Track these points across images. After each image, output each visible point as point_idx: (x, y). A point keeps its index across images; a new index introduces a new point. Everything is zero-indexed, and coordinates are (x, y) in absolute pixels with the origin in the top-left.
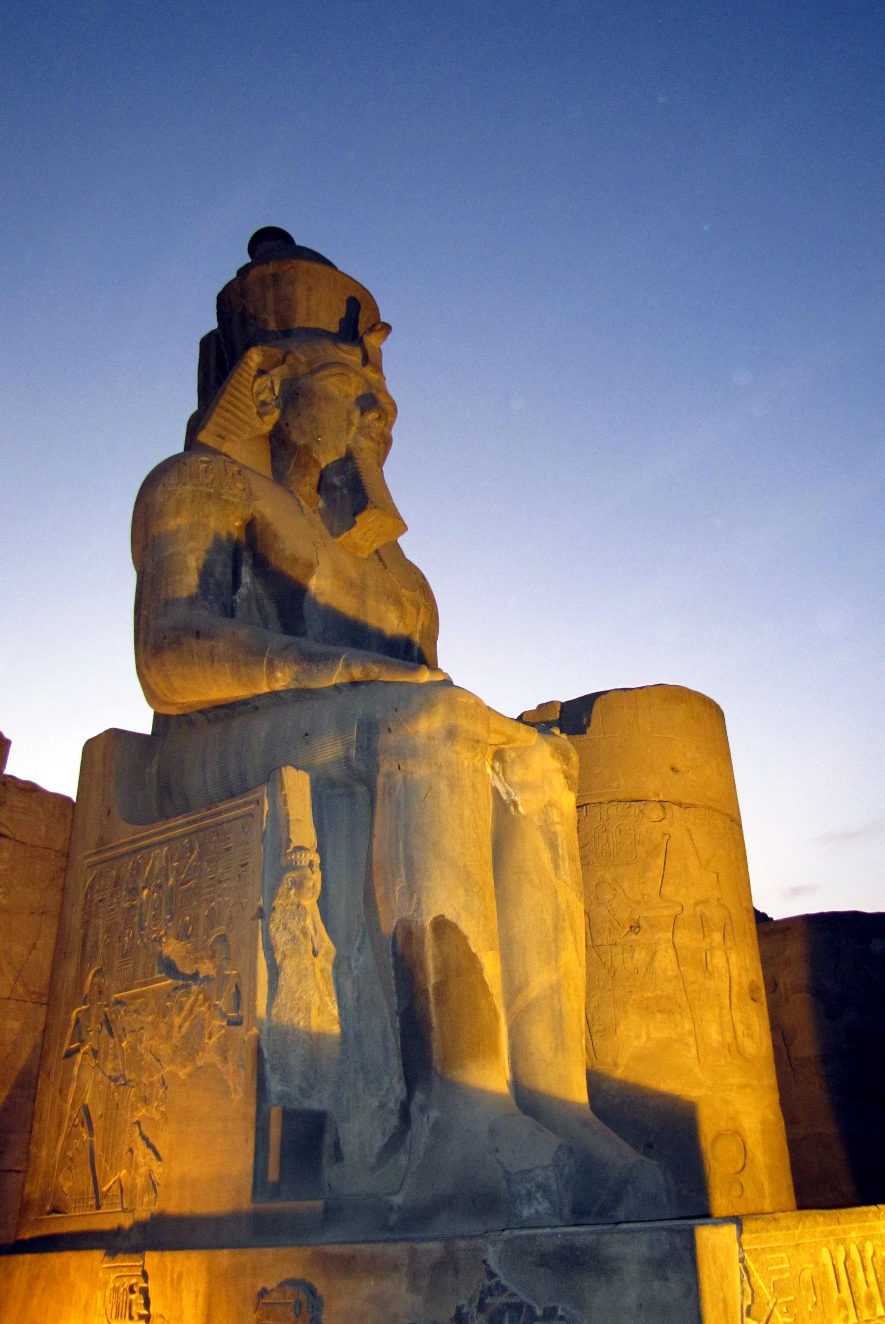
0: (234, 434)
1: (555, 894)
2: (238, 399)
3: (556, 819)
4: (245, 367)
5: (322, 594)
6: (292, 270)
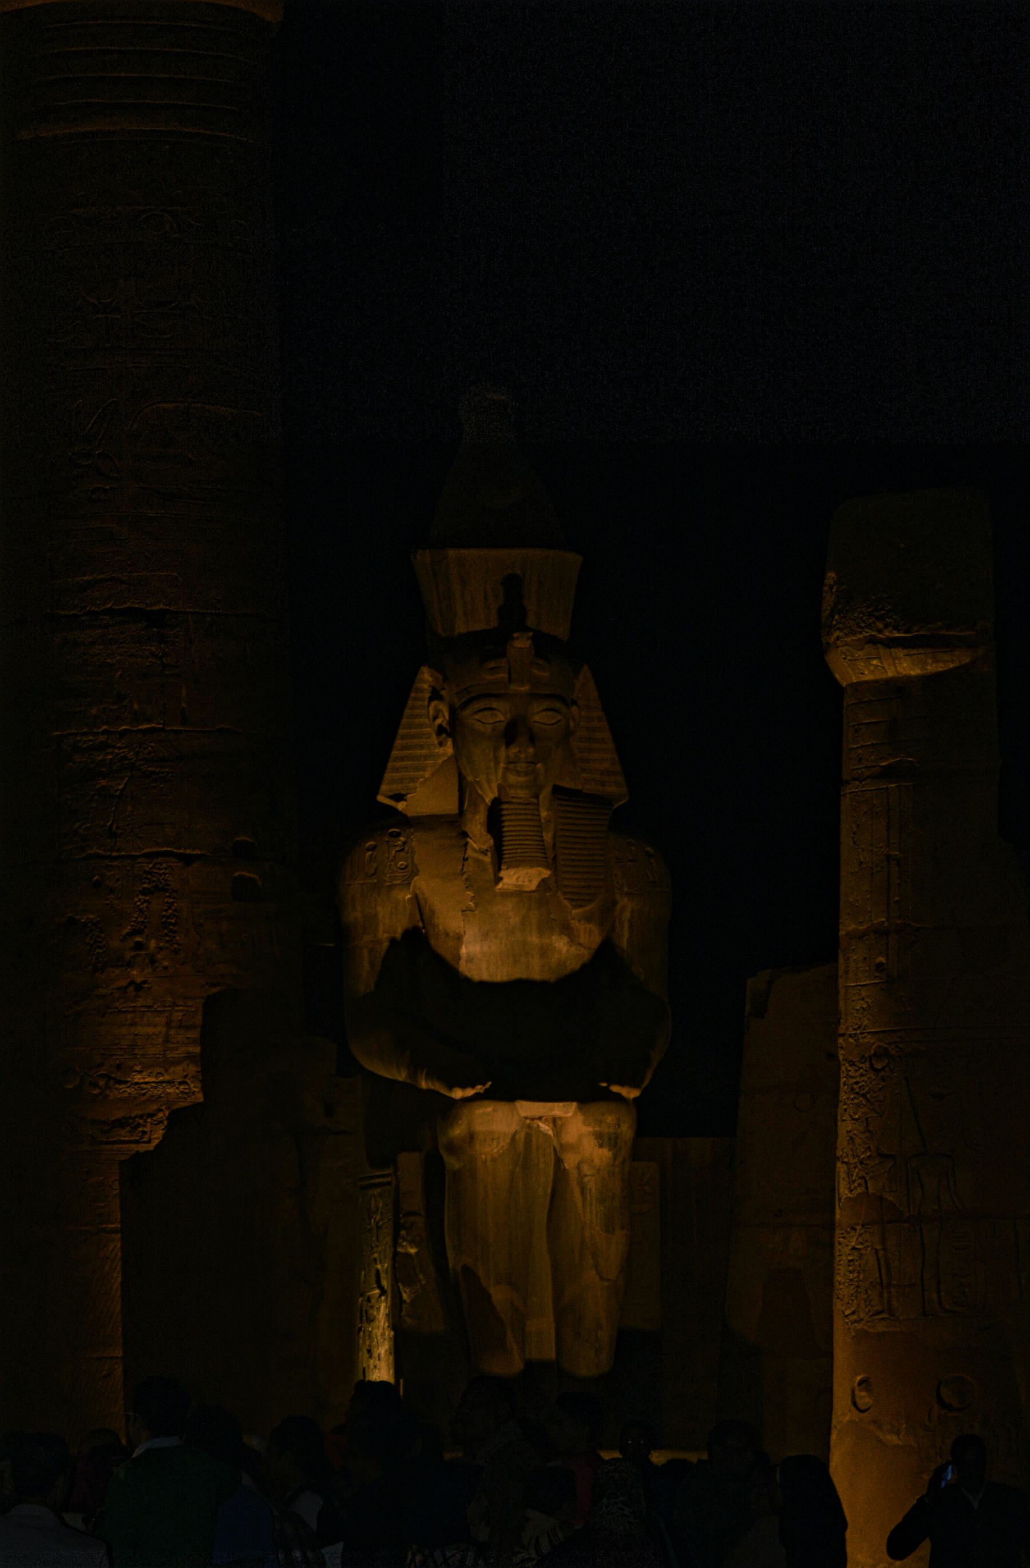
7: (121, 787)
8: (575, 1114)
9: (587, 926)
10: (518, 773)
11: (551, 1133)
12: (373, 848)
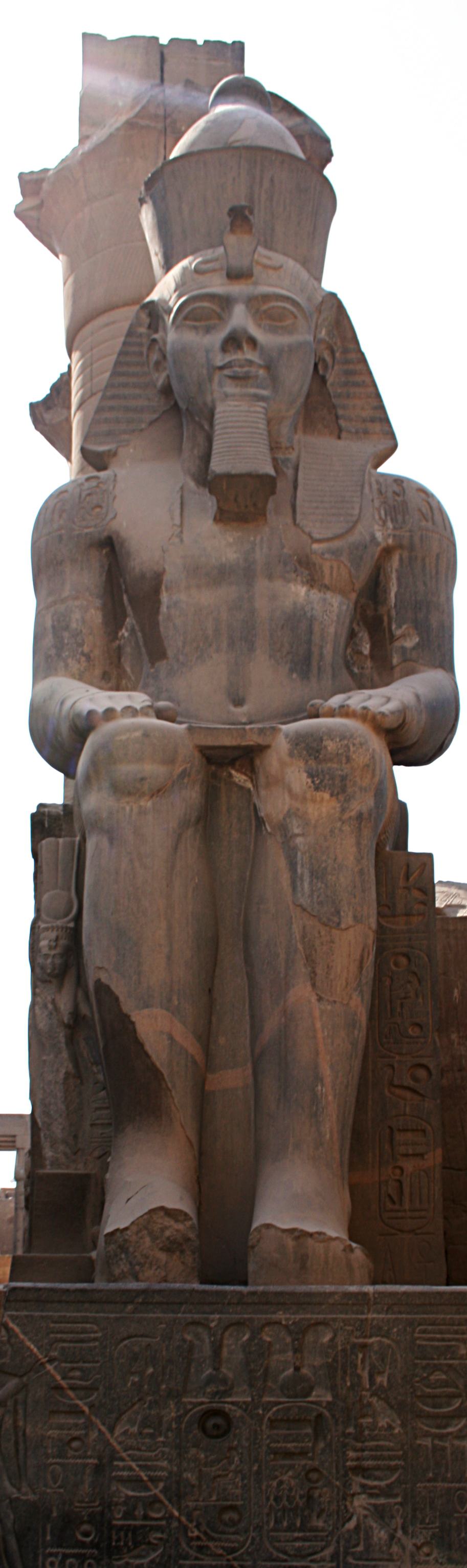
3: (297, 831)
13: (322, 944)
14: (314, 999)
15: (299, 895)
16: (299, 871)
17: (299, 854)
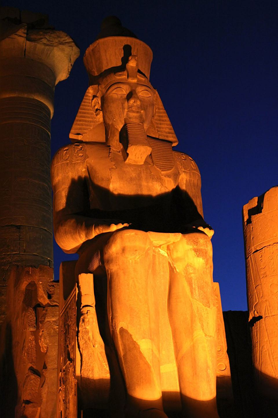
0: (85, 129)
1: (191, 305)
2: (85, 113)
3: (191, 272)
4: (87, 98)
5: (116, 190)
6: (98, 45)
7: (7, 268)
8: (181, 239)
9: (168, 179)
10: (133, 112)
11: (166, 255)
12: (67, 150)
13: (204, 314)
14: (204, 335)
15: (195, 296)
16: (194, 286)
17: (193, 280)
